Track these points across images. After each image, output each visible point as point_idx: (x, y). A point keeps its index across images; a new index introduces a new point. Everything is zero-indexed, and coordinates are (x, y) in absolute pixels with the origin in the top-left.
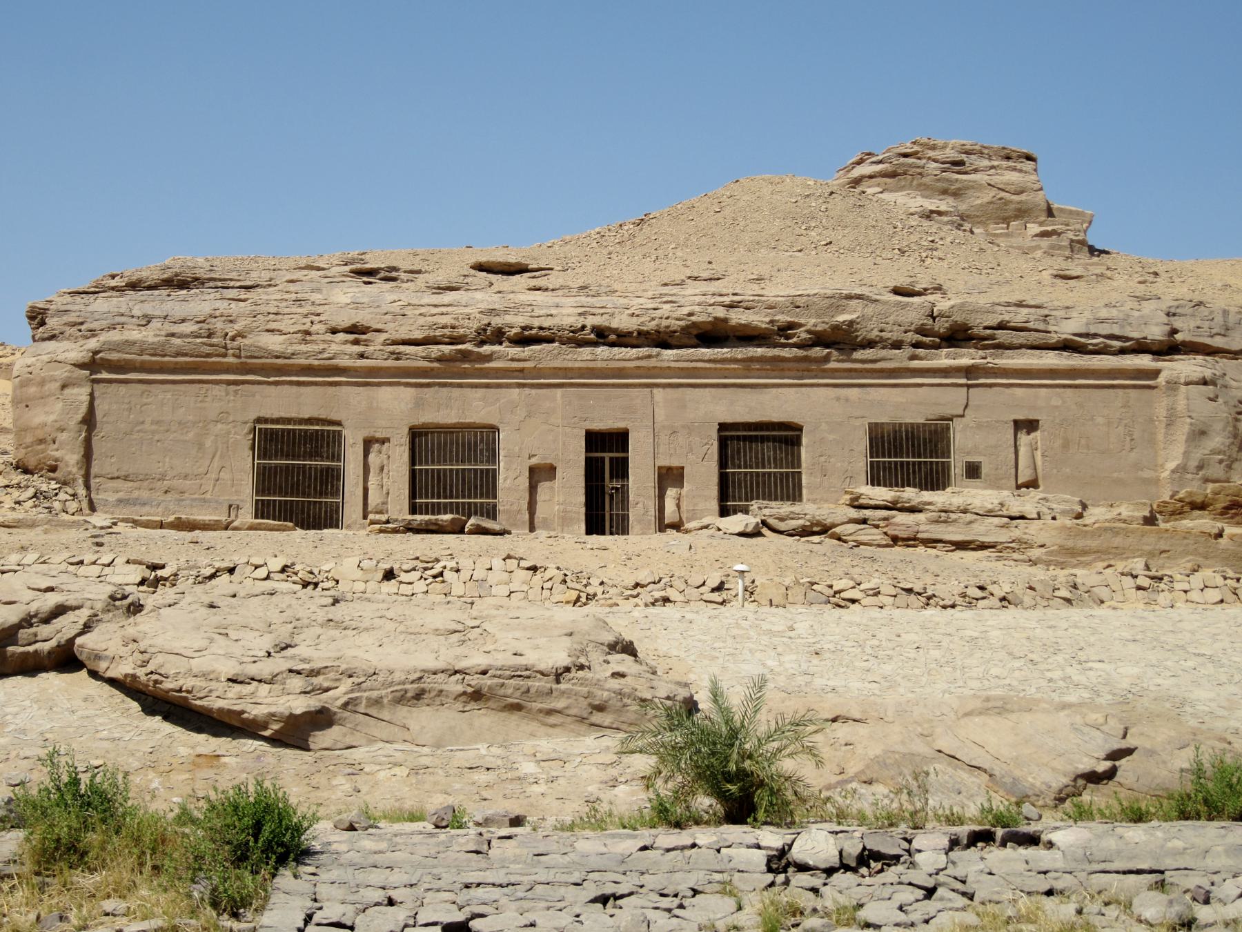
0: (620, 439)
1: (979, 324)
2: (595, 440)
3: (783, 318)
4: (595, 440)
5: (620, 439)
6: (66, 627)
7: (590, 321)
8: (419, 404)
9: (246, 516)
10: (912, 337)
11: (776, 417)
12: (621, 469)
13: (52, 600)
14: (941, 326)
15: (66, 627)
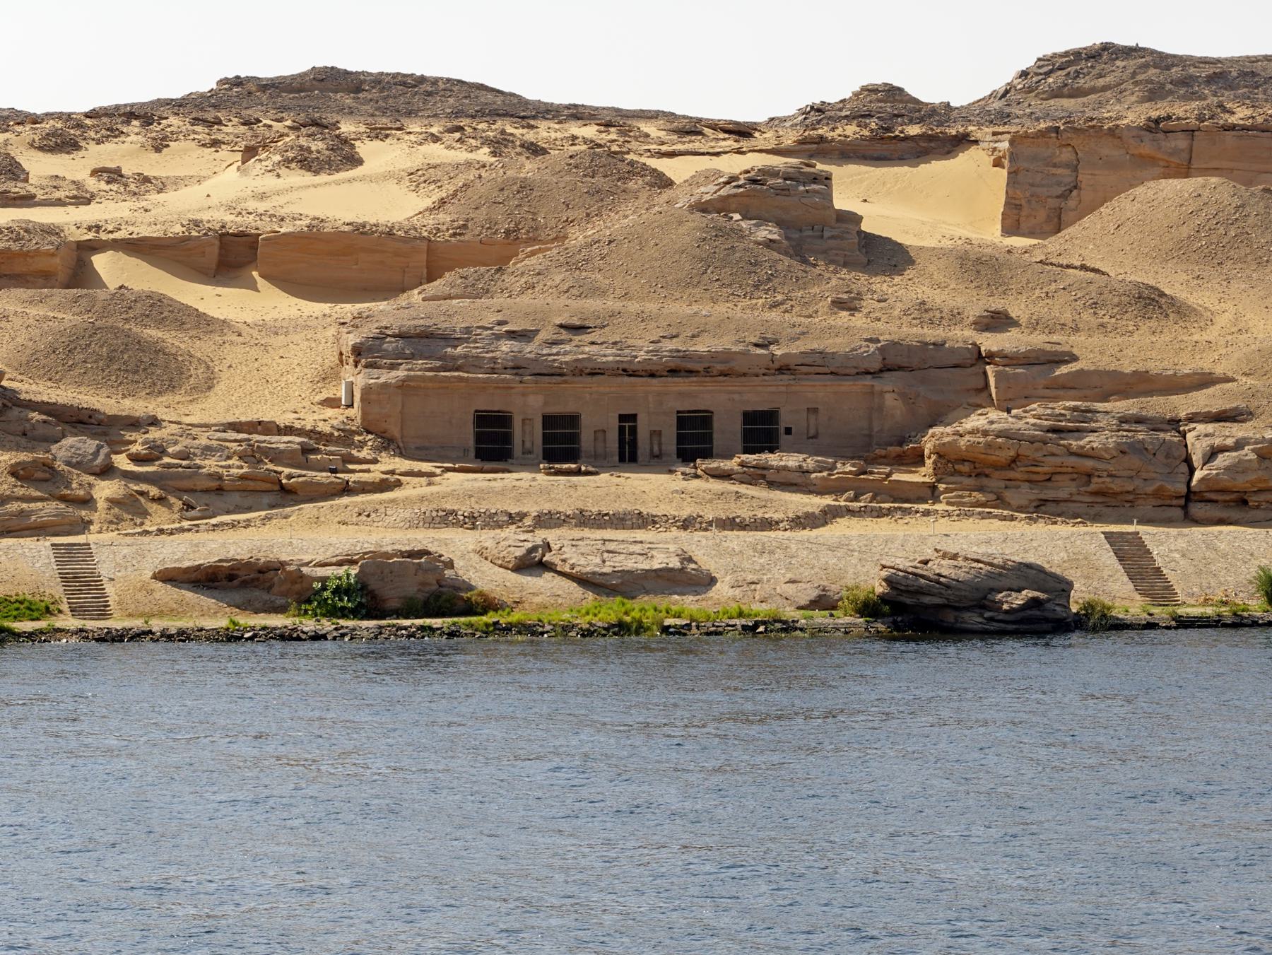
0: (633, 417)
1: (792, 363)
2: (623, 418)
3: (707, 365)
4: (623, 418)
5: (633, 417)
6: (538, 554)
7: (621, 366)
8: (546, 404)
9: (472, 454)
10: (764, 371)
11: (702, 408)
12: (633, 430)
13: (529, 545)
14: (777, 365)
15: (538, 554)
